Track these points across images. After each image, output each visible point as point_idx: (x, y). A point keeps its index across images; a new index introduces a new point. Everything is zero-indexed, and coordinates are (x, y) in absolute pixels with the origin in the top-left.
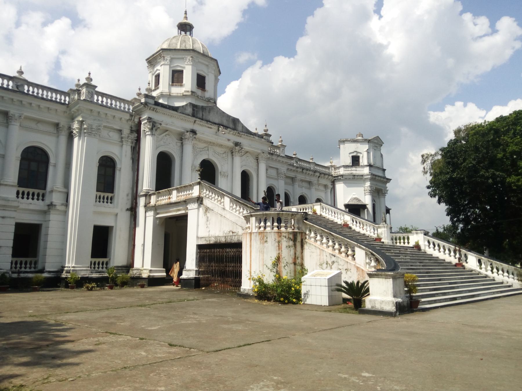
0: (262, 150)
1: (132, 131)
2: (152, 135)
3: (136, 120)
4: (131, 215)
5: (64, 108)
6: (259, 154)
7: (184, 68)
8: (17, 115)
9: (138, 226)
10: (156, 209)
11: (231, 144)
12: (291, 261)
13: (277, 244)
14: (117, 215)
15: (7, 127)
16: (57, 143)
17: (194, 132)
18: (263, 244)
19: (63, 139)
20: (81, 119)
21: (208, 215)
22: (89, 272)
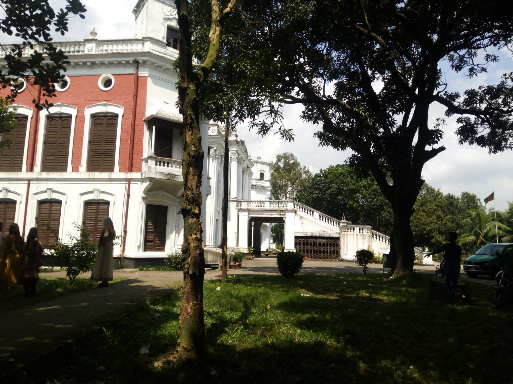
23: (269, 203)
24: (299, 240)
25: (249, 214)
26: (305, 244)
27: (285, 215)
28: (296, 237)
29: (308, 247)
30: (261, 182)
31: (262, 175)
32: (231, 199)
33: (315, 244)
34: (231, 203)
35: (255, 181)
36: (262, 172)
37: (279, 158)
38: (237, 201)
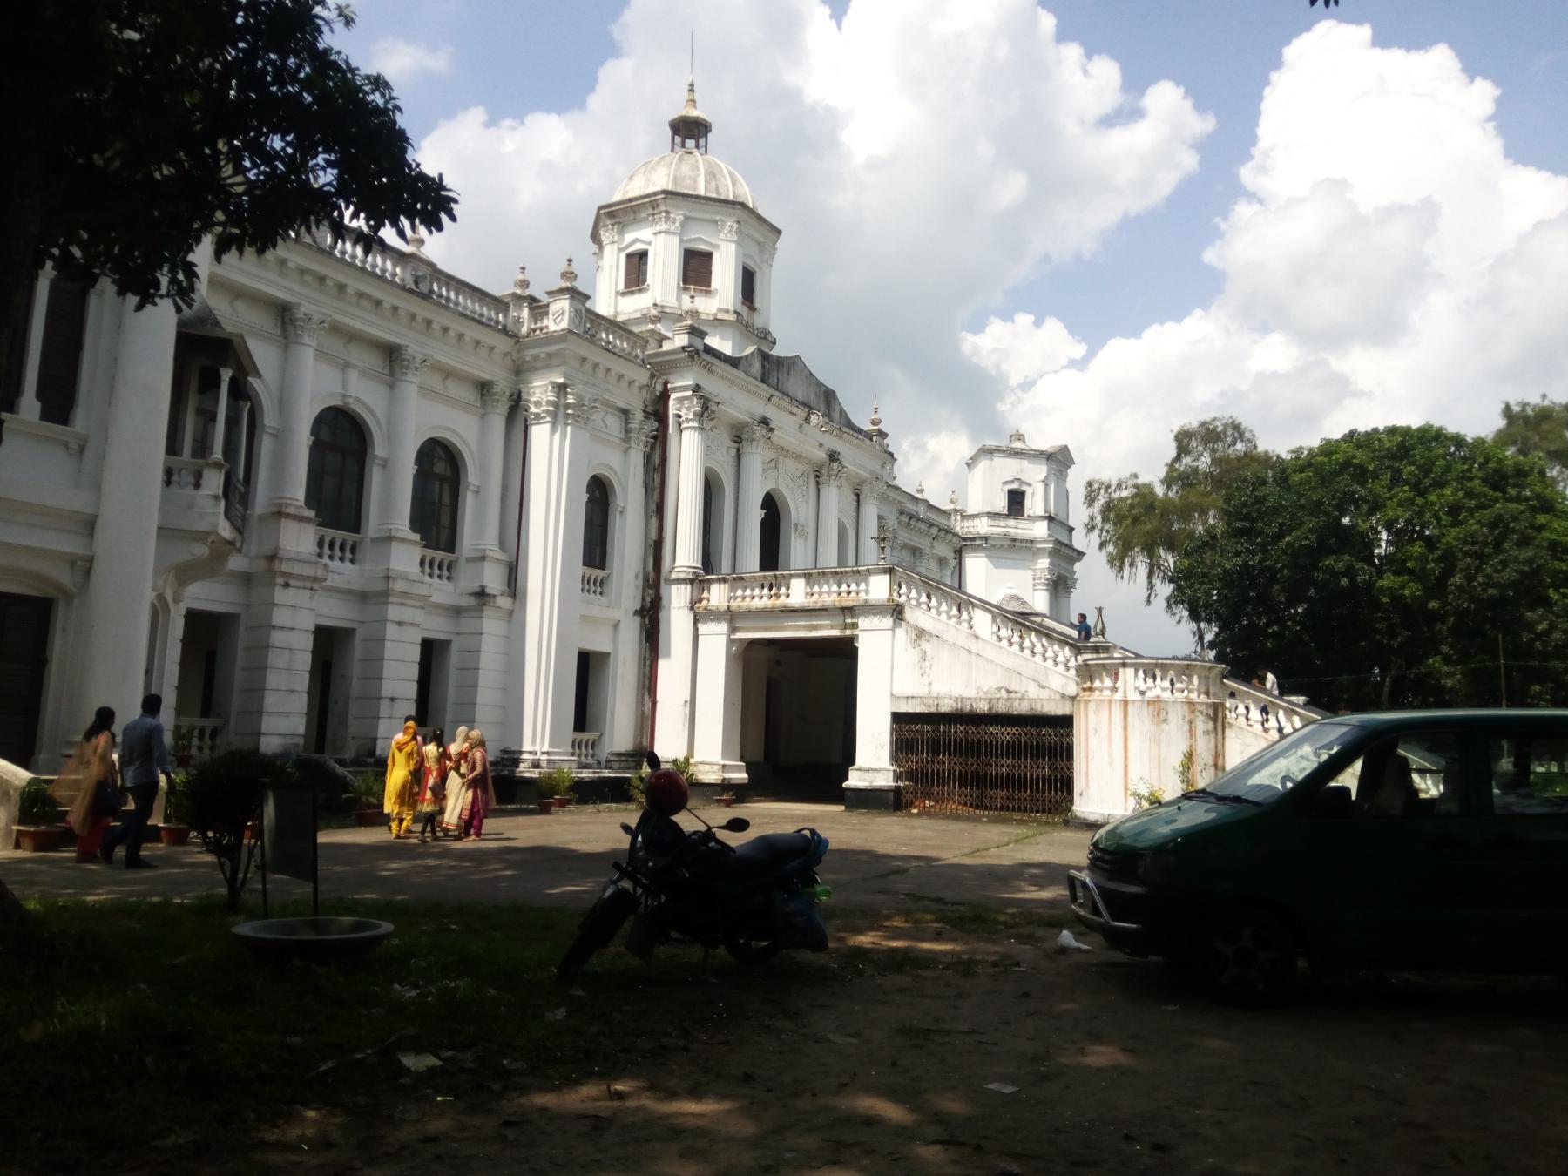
0: (872, 472)
1: (647, 414)
2: (701, 429)
3: (659, 388)
4: (643, 625)
5: (503, 344)
6: (863, 482)
7: (716, 247)
8: (419, 358)
9: (668, 655)
10: (731, 617)
11: (822, 455)
12: (1210, 761)
13: (1187, 727)
14: (616, 625)
15: (392, 386)
16: (483, 433)
17: (765, 422)
18: (1158, 724)
19: (498, 422)
20: (561, 380)
21: (925, 646)
22: (574, 765)
23: (802, 581)
24: (915, 732)
25: (733, 630)
26: (935, 747)
27: (854, 626)
28: (898, 719)
29: (945, 762)
30: (1011, 522)
31: (1016, 501)
32: (674, 576)
33: (970, 749)
34: (674, 588)
35: (985, 520)
36: (1015, 486)
37: (1183, 441)
38: (692, 582)
